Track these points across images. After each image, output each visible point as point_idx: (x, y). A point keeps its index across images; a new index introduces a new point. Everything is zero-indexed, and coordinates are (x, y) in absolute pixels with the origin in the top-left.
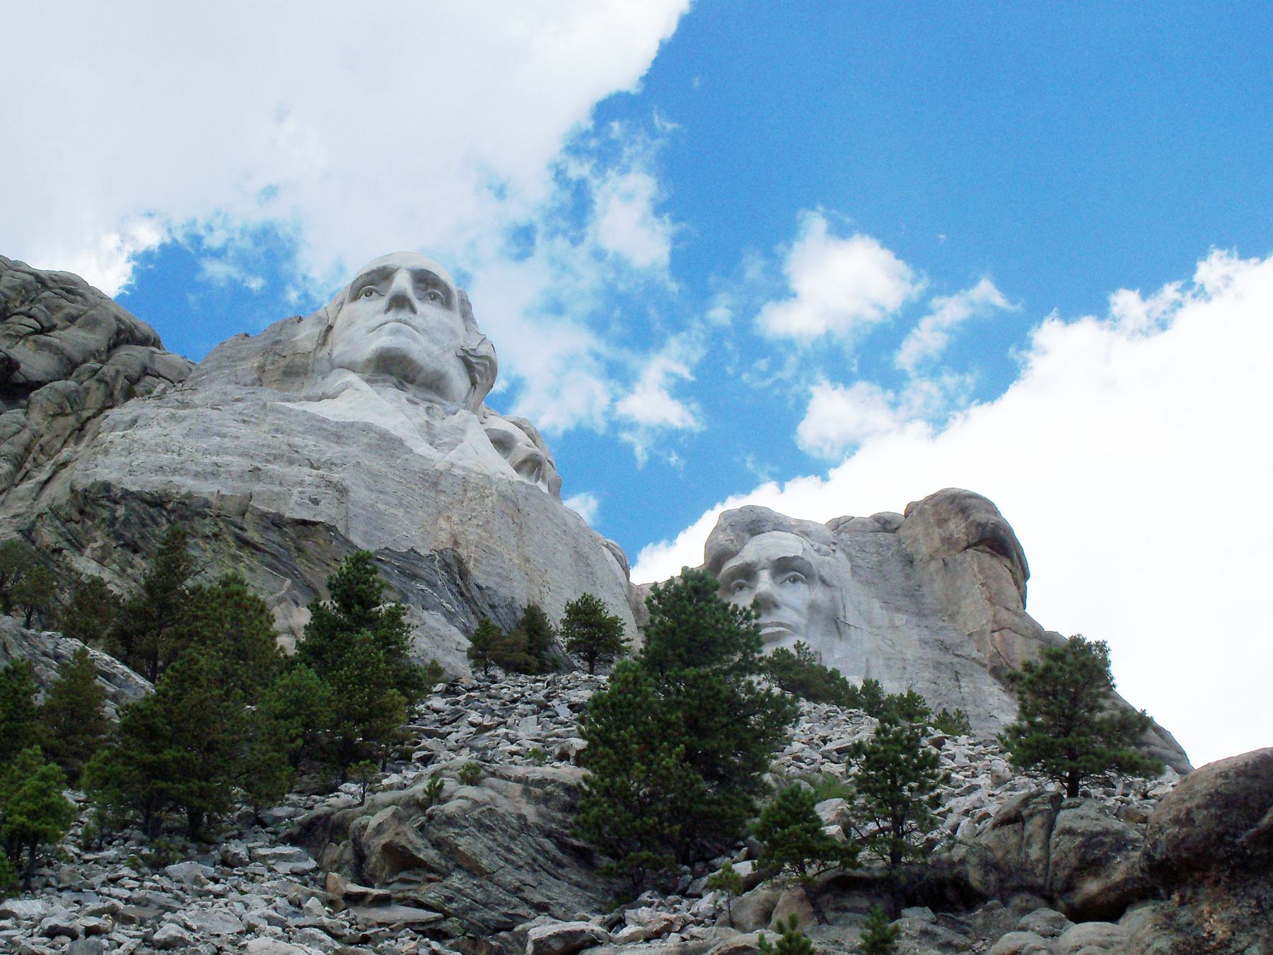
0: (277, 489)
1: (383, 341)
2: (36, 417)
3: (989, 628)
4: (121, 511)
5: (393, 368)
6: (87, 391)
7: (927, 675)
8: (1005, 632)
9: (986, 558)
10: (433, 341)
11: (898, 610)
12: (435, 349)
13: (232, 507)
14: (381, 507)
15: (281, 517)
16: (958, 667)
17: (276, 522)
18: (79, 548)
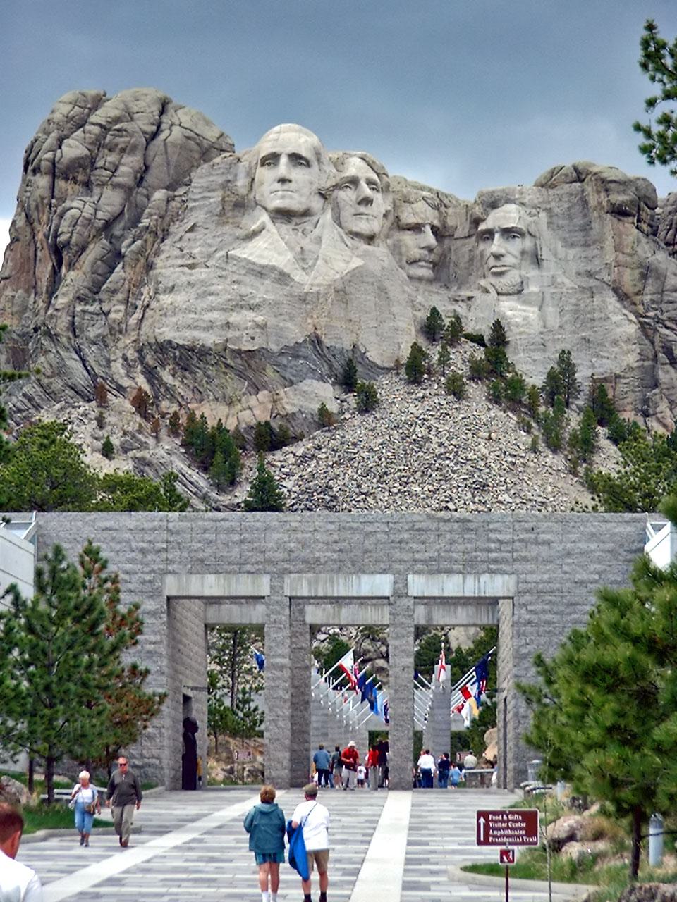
0: (237, 334)
1: (276, 203)
2: (128, 269)
3: (613, 264)
4: (177, 353)
5: (284, 215)
6: (146, 241)
7: (573, 301)
8: (620, 268)
9: (615, 220)
10: (301, 196)
11: (572, 245)
12: (303, 200)
13: (220, 348)
14: (281, 324)
15: (240, 350)
16: (594, 290)
17: (239, 353)
18: (163, 366)
